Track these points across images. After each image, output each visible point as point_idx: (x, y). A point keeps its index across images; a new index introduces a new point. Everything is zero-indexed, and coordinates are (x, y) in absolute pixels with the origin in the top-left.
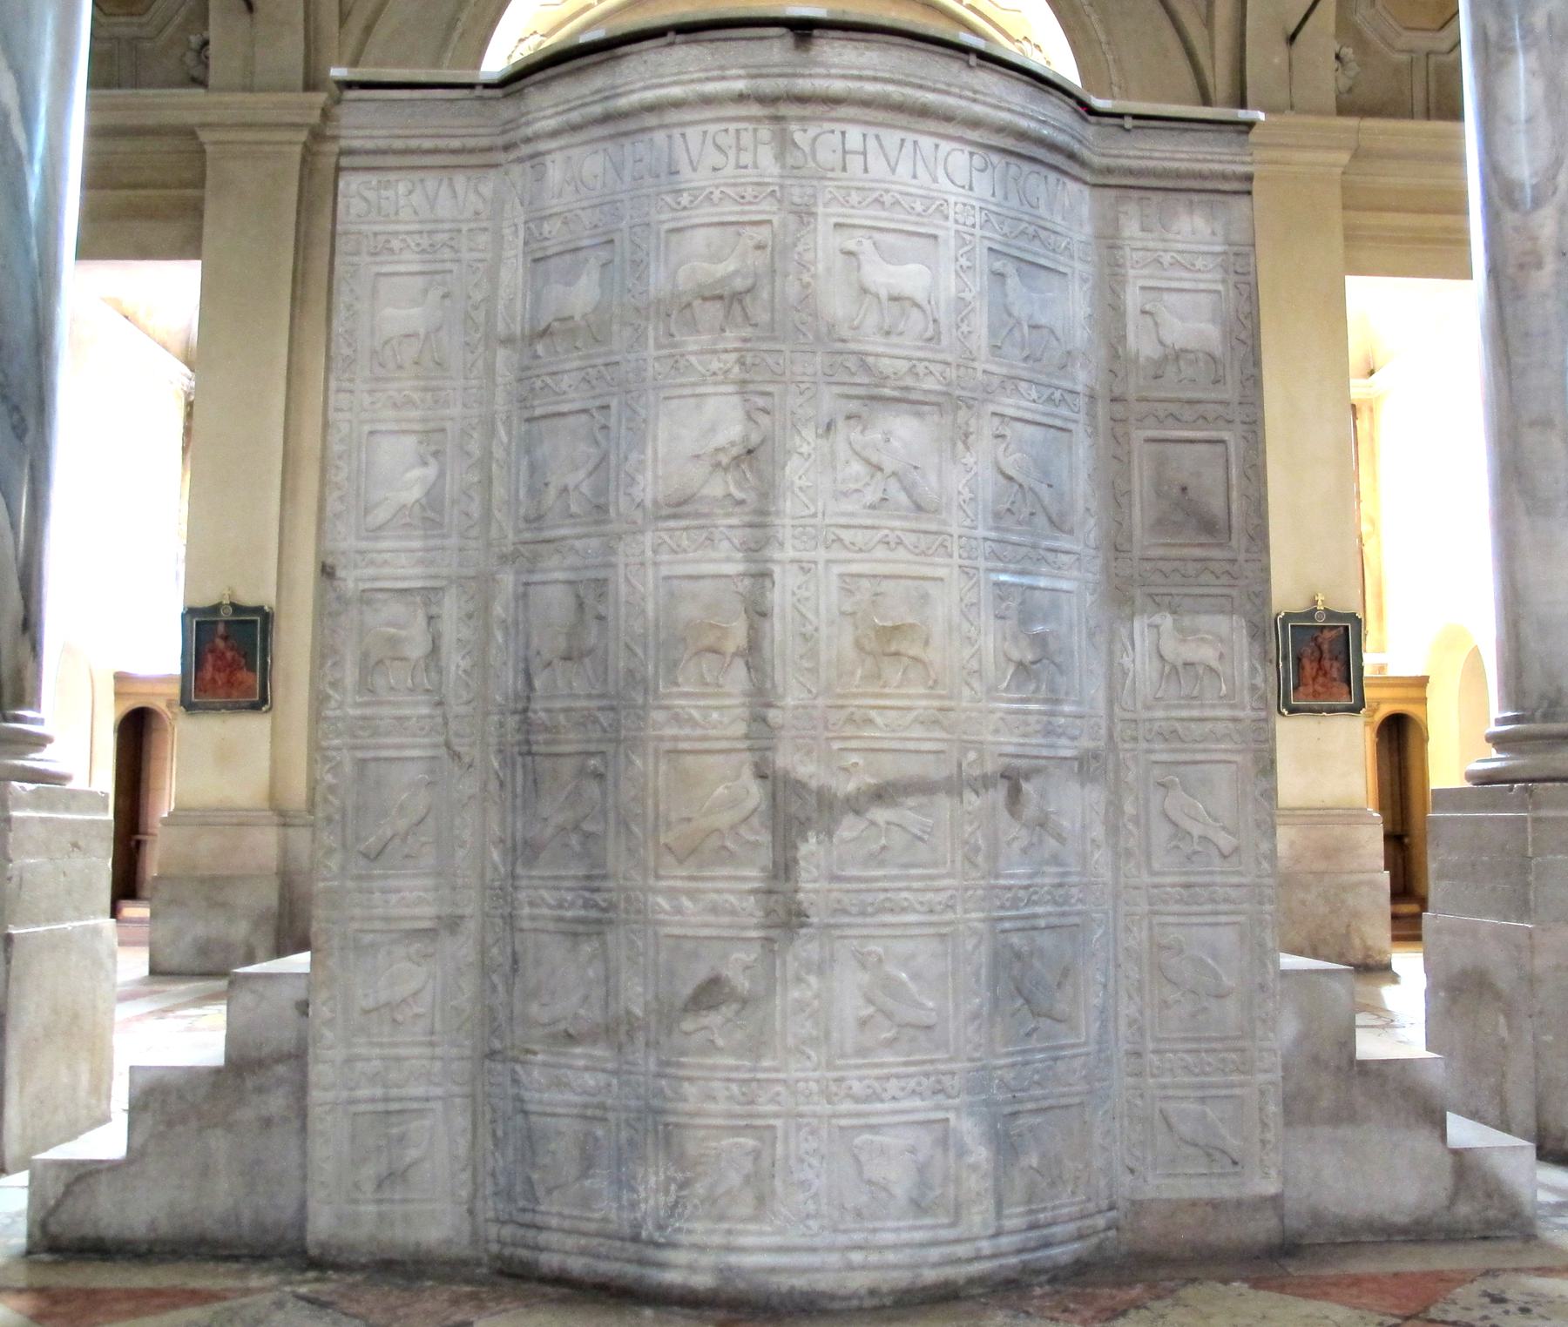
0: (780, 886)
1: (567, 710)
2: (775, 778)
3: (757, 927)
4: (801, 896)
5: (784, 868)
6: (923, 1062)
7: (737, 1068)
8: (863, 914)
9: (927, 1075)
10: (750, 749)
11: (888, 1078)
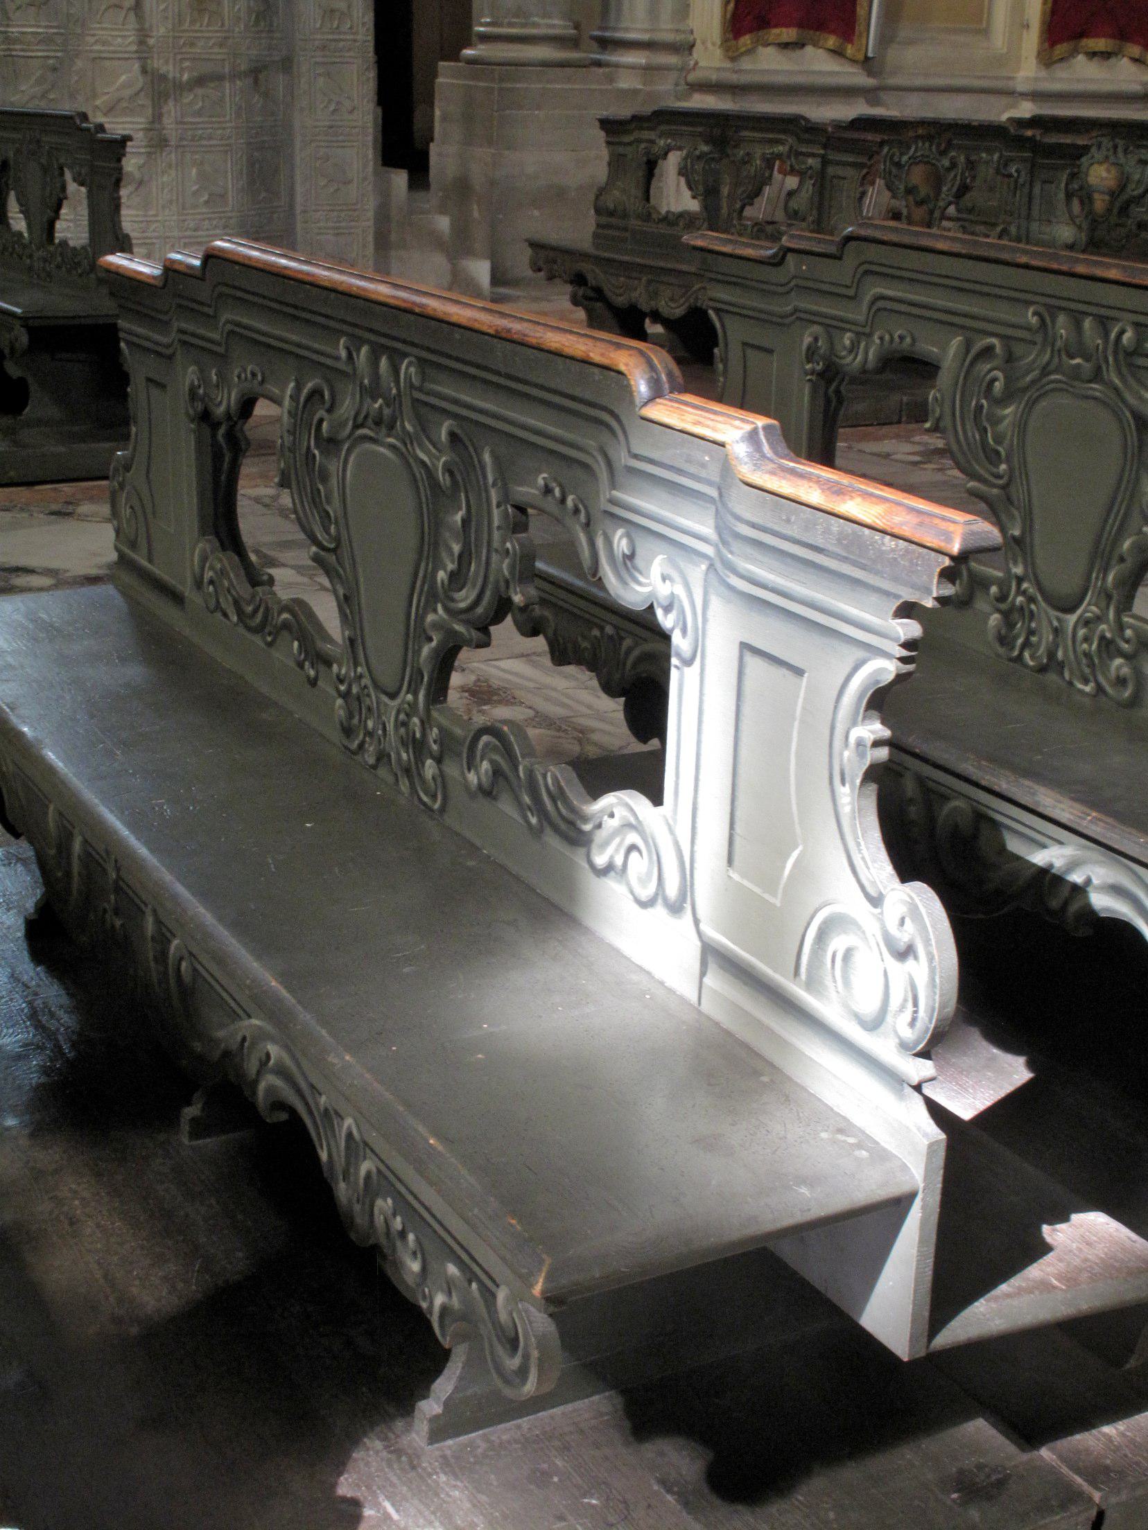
0: (157, 126)
1: (32, 33)
2: (153, 74)
3: (146, 147)
4: (164, 132)
5: (157, 117)
6: (220, 212)
7: (137, 216)
8: (192, 140)
9: (221, 218)
10: (139, 58)
11: (204, 220)
